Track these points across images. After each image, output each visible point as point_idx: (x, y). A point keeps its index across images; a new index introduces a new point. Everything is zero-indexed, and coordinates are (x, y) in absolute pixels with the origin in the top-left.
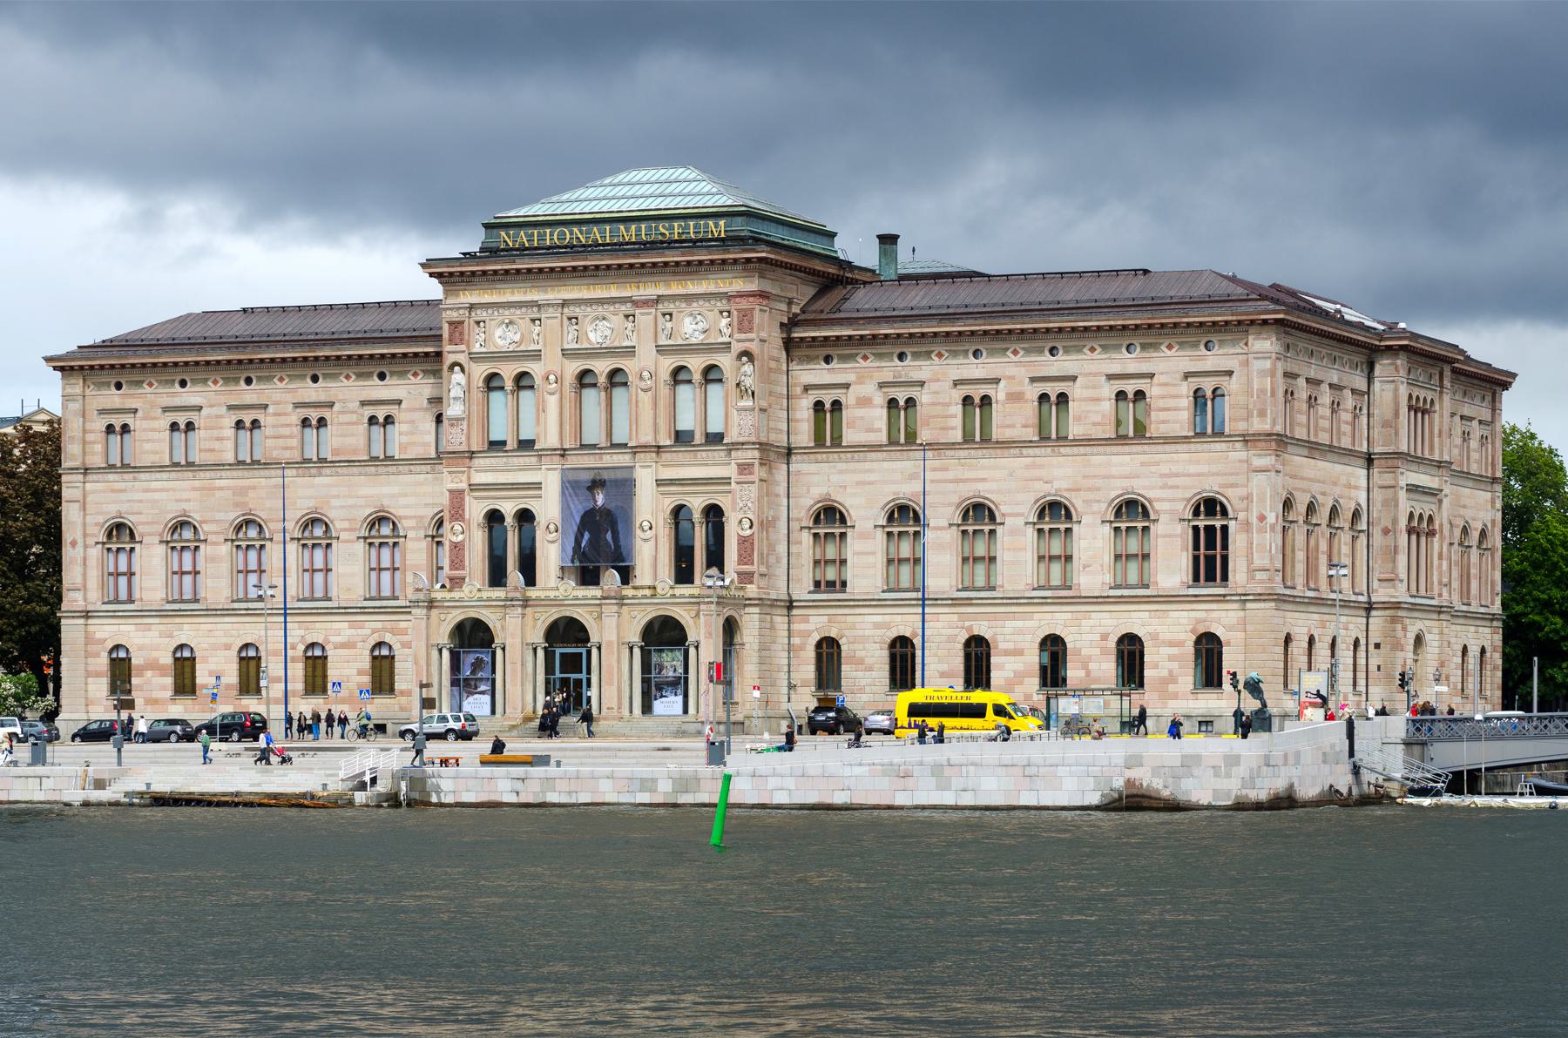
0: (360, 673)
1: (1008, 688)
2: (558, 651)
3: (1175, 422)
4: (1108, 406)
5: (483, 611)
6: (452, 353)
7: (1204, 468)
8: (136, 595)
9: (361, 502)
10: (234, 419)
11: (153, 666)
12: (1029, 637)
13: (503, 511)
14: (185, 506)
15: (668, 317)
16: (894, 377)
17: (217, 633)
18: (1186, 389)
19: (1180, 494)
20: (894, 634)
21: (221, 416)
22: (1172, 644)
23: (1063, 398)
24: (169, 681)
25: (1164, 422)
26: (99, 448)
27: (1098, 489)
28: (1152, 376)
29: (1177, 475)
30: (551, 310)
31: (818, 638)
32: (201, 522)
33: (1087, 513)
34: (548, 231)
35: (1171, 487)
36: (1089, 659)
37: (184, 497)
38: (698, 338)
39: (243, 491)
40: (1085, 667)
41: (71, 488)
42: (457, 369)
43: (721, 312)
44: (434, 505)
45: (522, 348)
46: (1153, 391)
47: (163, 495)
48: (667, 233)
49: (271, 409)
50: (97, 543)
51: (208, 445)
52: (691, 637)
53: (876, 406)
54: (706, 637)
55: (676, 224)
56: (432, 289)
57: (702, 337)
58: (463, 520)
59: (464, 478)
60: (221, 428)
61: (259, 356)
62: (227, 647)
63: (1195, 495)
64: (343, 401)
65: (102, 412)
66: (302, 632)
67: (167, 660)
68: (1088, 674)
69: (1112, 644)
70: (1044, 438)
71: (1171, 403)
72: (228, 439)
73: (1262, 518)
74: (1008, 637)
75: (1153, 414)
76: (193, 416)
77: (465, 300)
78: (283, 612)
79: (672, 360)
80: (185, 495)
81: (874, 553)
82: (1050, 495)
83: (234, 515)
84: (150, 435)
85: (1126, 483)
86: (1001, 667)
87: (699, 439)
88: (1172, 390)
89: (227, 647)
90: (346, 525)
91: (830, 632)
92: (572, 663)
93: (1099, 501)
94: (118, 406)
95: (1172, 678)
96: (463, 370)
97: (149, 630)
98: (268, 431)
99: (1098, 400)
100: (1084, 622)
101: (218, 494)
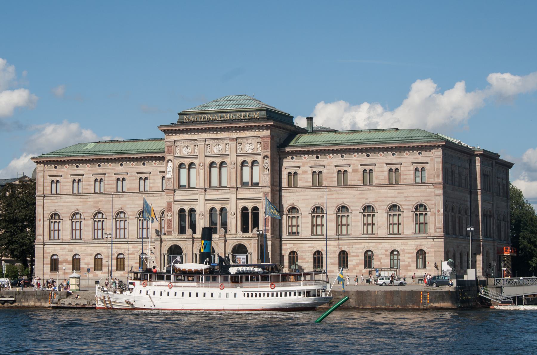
0: (136, 263)
1: (355, 267)
3: (409, 179)
4: (386, 174)
5: (179, 242)
6: (169, 156)
7: (419, 194)
8: (60, 237)
9: (137, 206)
10: (94, 178)
11: (66, 261)
12: (361, 251)
13: (185, 209)
14: (77, 207)
15: (240, 144)
16: (315, 164)
17: (88, 250)
18: (412, 168)
19: (411, 203)
21: (90, 178)
22: (409, 253)
23: (371, 171)
24: (71, 266)
25: (405, 179)
26: (49, 188)
27: (383, 201)
28: (401, 164)
29: (410, 197)
30: (201, 142)
31: (290, 251)
32: (83, 213)
33: (380, 209)
34: (200, 116)
35: (408, 201)
36: (381, 258)
37: (78, 204)
38: (250, 151)
39: (97, 202)
40: (380, 261)
41: (39, 201)
42: (170, 161)
43: (258, 143)
44: (161, 207)
45: (192, 154)
46: (401, 168)
47: (70, 204)
48: (239, 116)
50: (48, 220)
51: (85, 187)
52: (249, 251)
53: (309, 174)
54: (254, 251)
55: (242, 114)
56: (162, 135)
57: (252, 151)
59: (173, 197)
60: (90, 181)
61: (103, 158)
62: (91, 255)
63: (416, 203)
64: (131, 172)
65: (50, 176)
67: (70, 259)
68: (381, 263)
70: (364, 184)
71: (407, 173)
73: (439, 211)
74: (354, 251)
75: (401, 176)
77: (172, 139)
79: (241, 159)
80: (77, 204)
81: (308, 223)
82: (367, 203)
83: (94, 211)
84: (66, 184)
85: (393, 199)
86: (352, 261)
87: (250, 184)
88: (408, 168)
89: (91, 255)
90: (131, 214)
91: (294, 249)
93: (383, 205)
95: (409, 265)
96: (172, 161)
97: (65, 249)
98: (106, 182)
99: (383, 172)
100: (379, 246)
101: (89, 203)
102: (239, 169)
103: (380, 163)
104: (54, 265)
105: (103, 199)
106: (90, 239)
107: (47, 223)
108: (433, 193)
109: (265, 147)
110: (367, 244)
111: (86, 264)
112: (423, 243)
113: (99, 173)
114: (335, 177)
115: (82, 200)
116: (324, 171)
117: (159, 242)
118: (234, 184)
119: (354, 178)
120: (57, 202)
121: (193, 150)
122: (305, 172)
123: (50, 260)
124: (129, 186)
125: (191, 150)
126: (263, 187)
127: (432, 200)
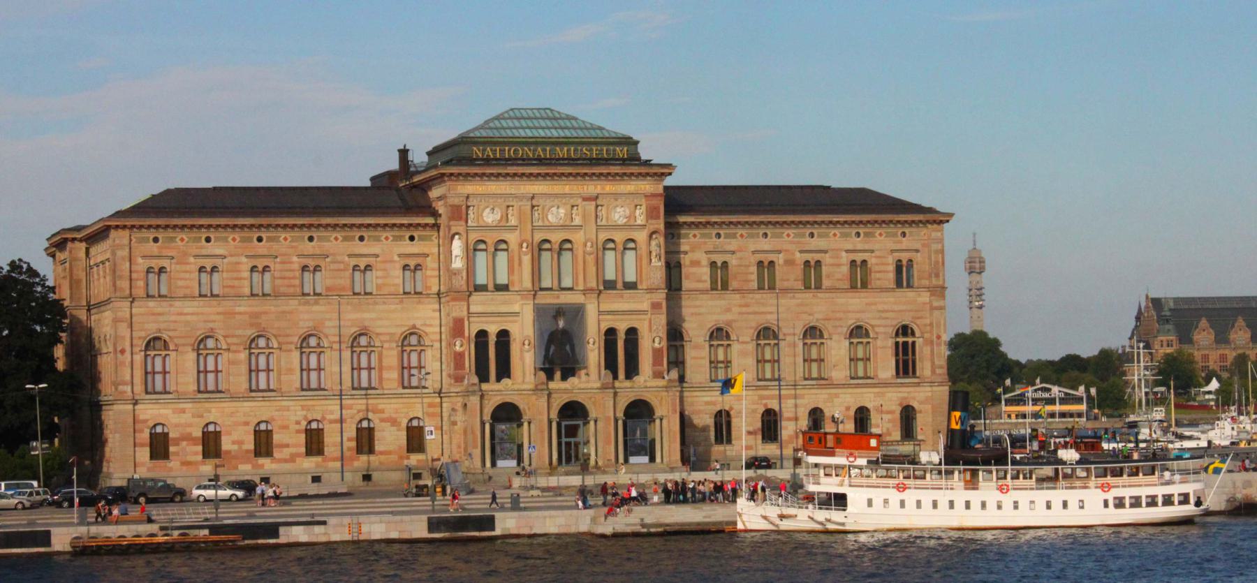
2: (563, 424)
4: (845, 269)
7: (904, 308)
10: (250, 265)
11: (188, 438)
14: (211, 325)
16: (714, 248)
17: (238, 414)
18: (891, 260)
19: (889, 322)
20: (718, 408)
23: (818, 263)
24: (200, 448)
25: (879, 279)
26: (141, 284)
27: (841, 319)
28: (872, 251)
34: (507, 148)
38: (622, 221)
42: (457, 237)
43: (636, 206)
45: (501, 224)
46: (872, 261)
47: (194, 318)
49: (278, 260)
51: (230, 283)
53: (703, 266)
57: (625, 220)
58: (464, 337)
59: (465, 308)
62: (247, 424)
64: (334, 255)
66: (304, 413)
67: (198, 433)
69: (852, 413)
70: (807, 287)
71: (882, 268)
72: (245, 279)
75: (873, 274)
76: (218, 262)
77: (461, 192)
78: (338, 397)
80: (213, 317)
83: (251, 332)
84: (183, 275)
85: (858, 315)
86: (786, 428)
87: (620, 285)
89: (247, 424)
92: (572, 432)
93: (841, 327)
94: (157, 254)
97: (184, 412)
99: (839, 265)
100: (835, 400)
102: (600, 254)
103: (833, 250)
104: (160, 446)
105: (271, 307)
106: (242, 391)
107: (139, 358)
108: (928, 307)
109: (651, 214)
110: (814, 396)
111: (234, 443)
112: (912, 395)
113: (261, 254)
114: (752, 273)
115: (220, 309)
116: (733, 261)
117: (479, 399)
118: (593, 284)
119: (788, 276)
120: (160, 314)
121: (505, 215)
122: (696, 263)
123: (148, 435)
124: (329, 282)
125: (499, 214)
126: (650, 290)
127: (926, 318)
